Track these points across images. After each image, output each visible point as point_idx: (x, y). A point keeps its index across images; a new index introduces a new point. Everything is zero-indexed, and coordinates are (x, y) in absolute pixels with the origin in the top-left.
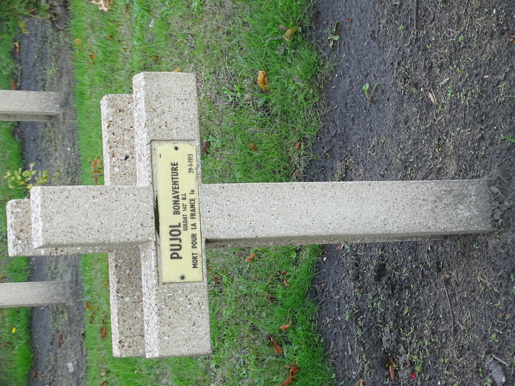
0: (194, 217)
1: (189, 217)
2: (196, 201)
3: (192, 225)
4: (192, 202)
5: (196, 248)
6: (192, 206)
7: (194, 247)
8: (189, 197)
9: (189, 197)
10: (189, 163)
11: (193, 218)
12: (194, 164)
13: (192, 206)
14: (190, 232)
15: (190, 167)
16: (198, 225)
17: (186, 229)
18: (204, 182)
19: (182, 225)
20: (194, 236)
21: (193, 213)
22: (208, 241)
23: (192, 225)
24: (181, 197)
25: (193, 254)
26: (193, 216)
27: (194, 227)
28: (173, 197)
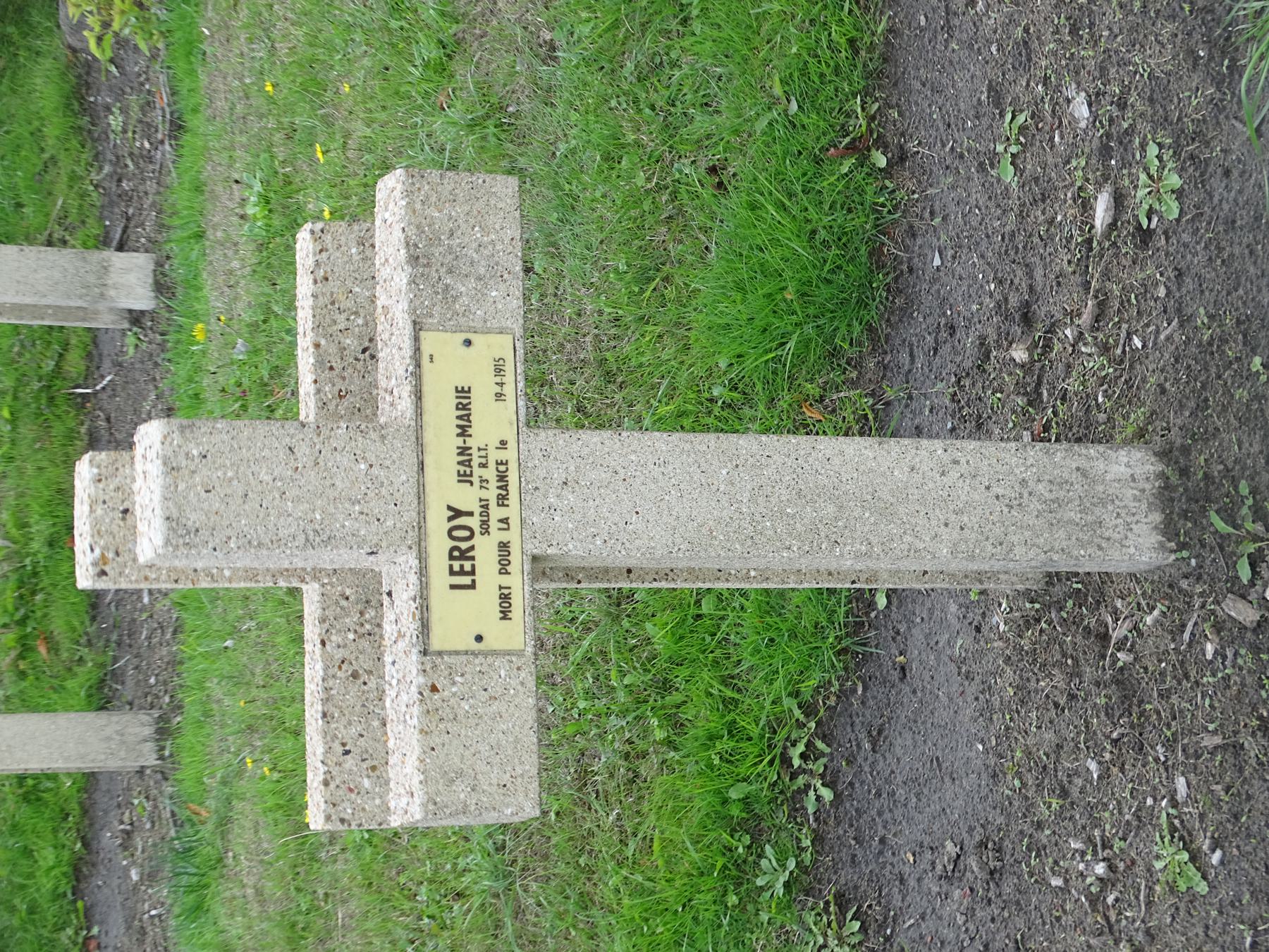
2: (513, 466)
3: (501, 521)
5: (507, 573)
6: (502, 477)
7: (504, 571)
8: (494, 455)
9: (494, 455)
10: (498, 379)
11: (503, 505)
12: (509, 378)
13: (502, 477)
14: (496, 536)
15: (498, 389)
16: (515, 522)
20: (504, 546)
21: (504, 493)
23: (501, 521)
25: (500, 588)
28: (459, 463)
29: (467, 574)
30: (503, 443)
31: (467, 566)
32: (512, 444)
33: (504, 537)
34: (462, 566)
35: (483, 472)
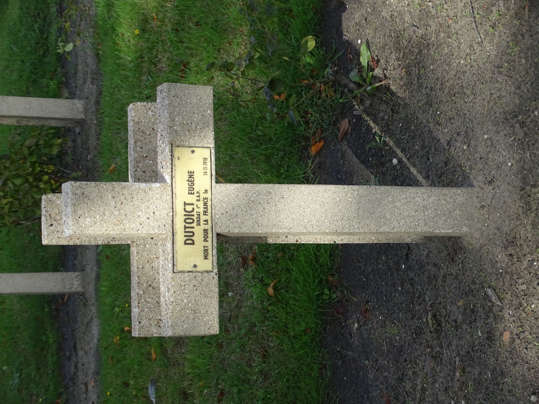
1: (202, 213)
3: (204, 221)
5: (207, 241)
7: (205, 240)
8: (203, 196)
9: (203, 196)
10: (204, 166)
11: (206, 215)
13: (205, 204)
16: (210, 222)
17: (199, 224)
18: (217, 182)
19: (195, 221)
23: (204, 221)
25: (204, 247)
26: (205, 213)
32: (209, 191)
33: (206, 227)
35: (198, 203)
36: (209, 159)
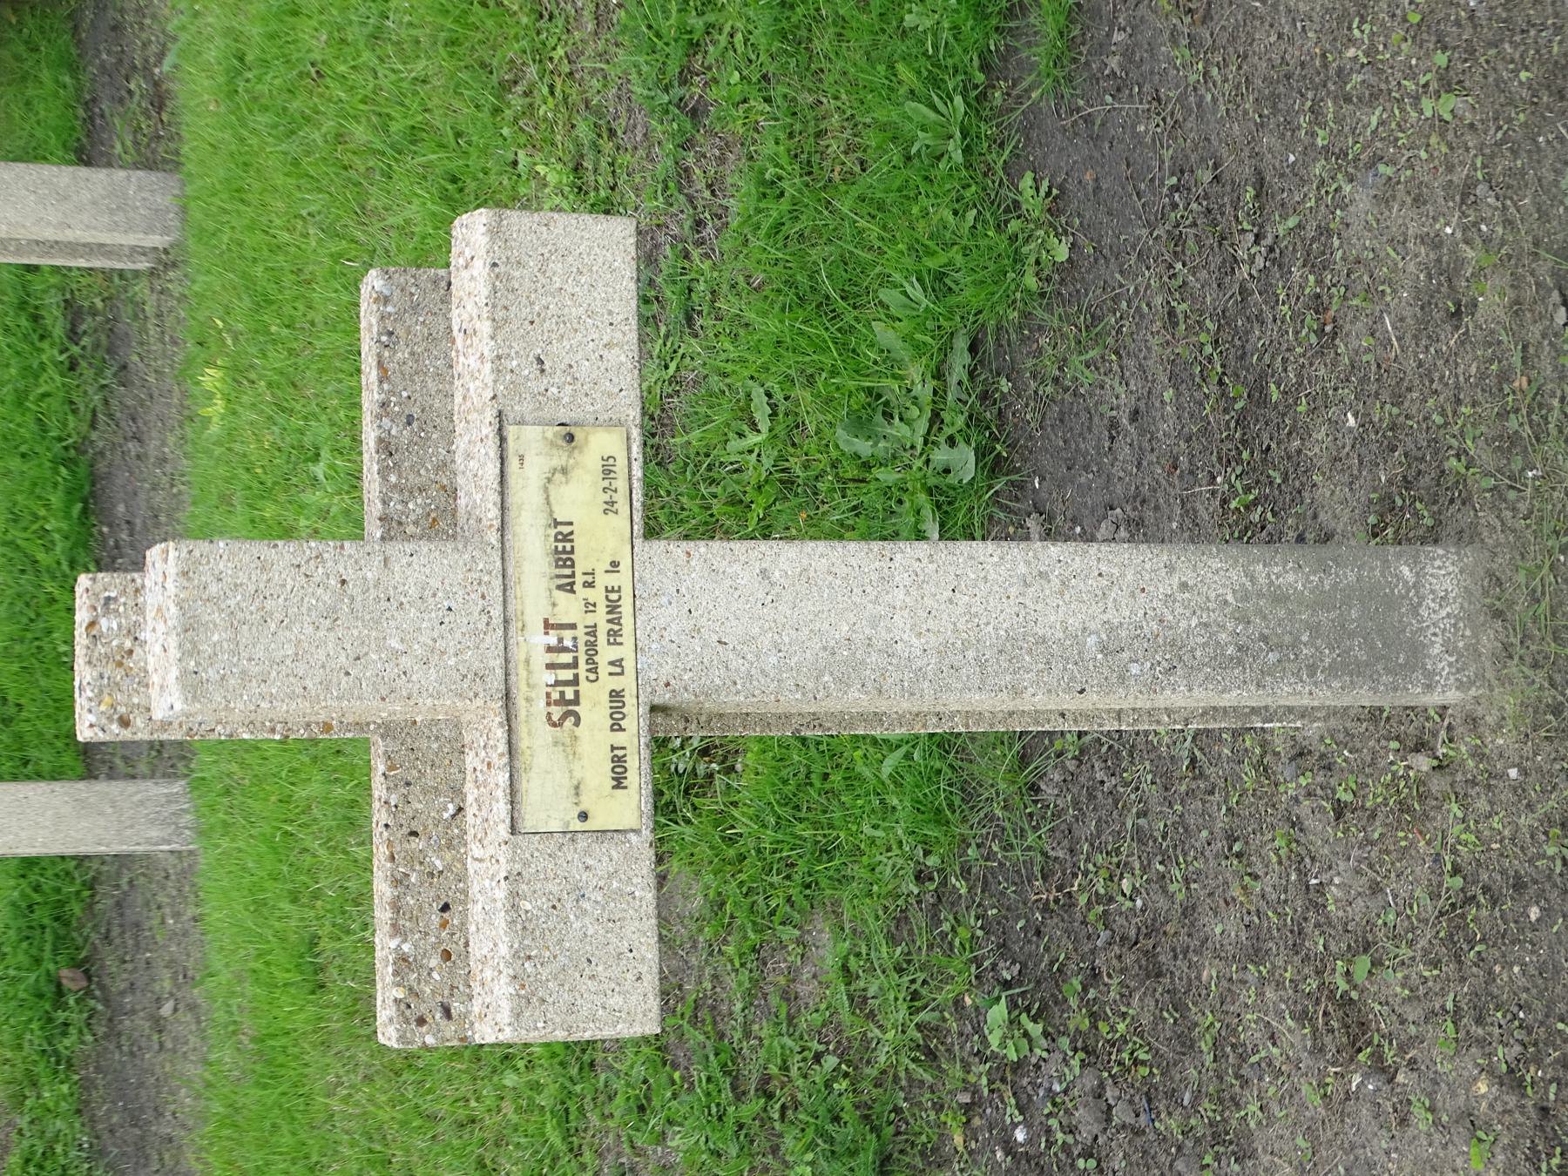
0: (619, 640)
3: (612, 663)
4: (614, 596)
5: (622, 729)
6: (613, 608)
7: (616, 727)
8: (603, 580)
11: (616, 643)
13: (613, 608)
15: (606, 497)
16: (629, 665)
21: (616, 628)
22: (654, 709)
23: (612, 663)
24: (580, 579)
25: (613, 748)
27: (618, 670)
29: (570, 703)
30: (615, 564)
31: (570, 695)
34: (562, 693)
36: (622, 462)
